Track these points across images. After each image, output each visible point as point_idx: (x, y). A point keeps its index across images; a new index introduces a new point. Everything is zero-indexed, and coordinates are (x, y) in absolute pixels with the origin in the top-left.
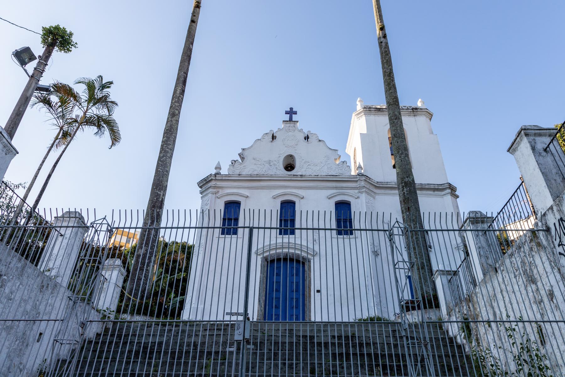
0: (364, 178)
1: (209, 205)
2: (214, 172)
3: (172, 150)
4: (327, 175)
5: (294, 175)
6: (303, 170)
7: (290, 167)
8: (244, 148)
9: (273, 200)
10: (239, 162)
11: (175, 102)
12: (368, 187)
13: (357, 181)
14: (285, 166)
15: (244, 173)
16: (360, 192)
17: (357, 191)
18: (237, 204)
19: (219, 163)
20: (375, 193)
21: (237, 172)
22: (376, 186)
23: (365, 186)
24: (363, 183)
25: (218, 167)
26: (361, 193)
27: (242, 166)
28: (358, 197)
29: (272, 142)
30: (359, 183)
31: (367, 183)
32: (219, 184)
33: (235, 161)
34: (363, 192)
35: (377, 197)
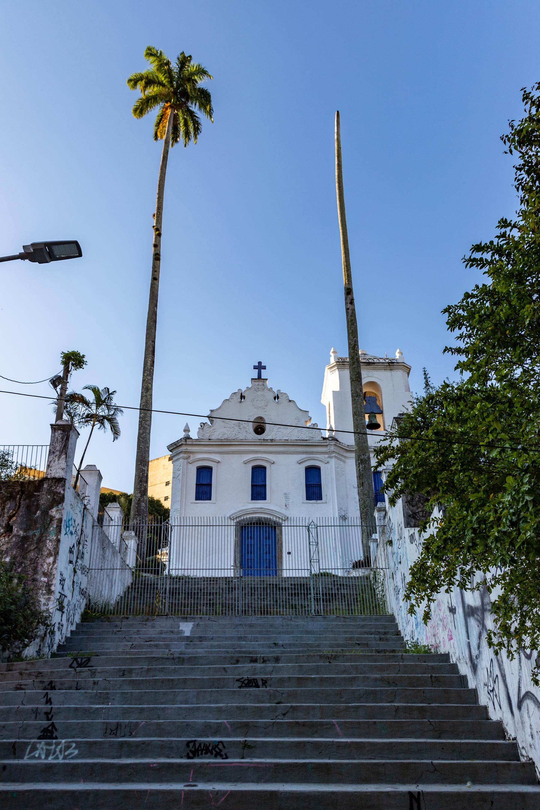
0: (334, 443)
1: (181, 471)
2: (182, 435)
3: (150, 425)
4: (297, 439)
5: (264, 440)
6: (273, 433)
7: (260, 429)
8: (212, 409)
9: (243, 465)
10: (208, 425)
11: (147, 375)
12: (338, 452)
13: (327, 446)
14: (255, 427)
15: (213, 437)
16: (329, 457)
17: (327, 456)
18: (209, 469)
19: (187, 425)
20: (345, 457)
21: (207, 436)
22: (346, 450)
23: (335, 450)
24: (332, 448)
25: (187, 430)
26: (331, 458)
27: (211, 429)
28: (328, 462)
29: (241, 402)
30: (329, 447)
31: (336, 448)
32: (190, 448)
33: (204, 424)
34: (333, 456)
35: (347, 461)
